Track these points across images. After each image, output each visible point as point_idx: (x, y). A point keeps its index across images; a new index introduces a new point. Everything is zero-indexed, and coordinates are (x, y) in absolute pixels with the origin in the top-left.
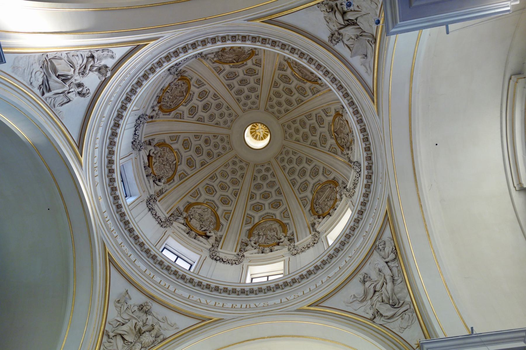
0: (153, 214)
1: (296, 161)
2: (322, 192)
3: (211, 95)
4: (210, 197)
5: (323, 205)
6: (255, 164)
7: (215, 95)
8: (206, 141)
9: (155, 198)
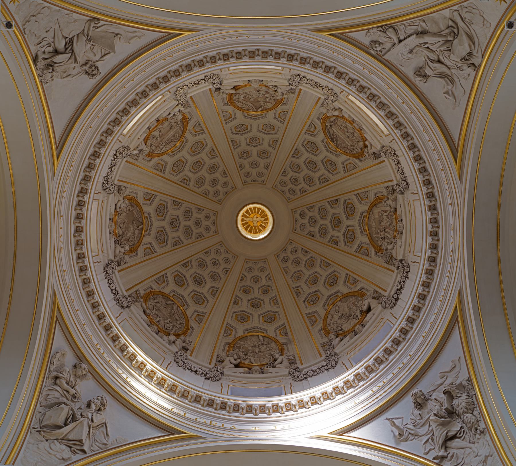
0: (313, 375)
1: (296, 172)
3: (182, 270)
5: (354, 139)
6: (293, 232)
7: (185, 265)
9: (294, 368)
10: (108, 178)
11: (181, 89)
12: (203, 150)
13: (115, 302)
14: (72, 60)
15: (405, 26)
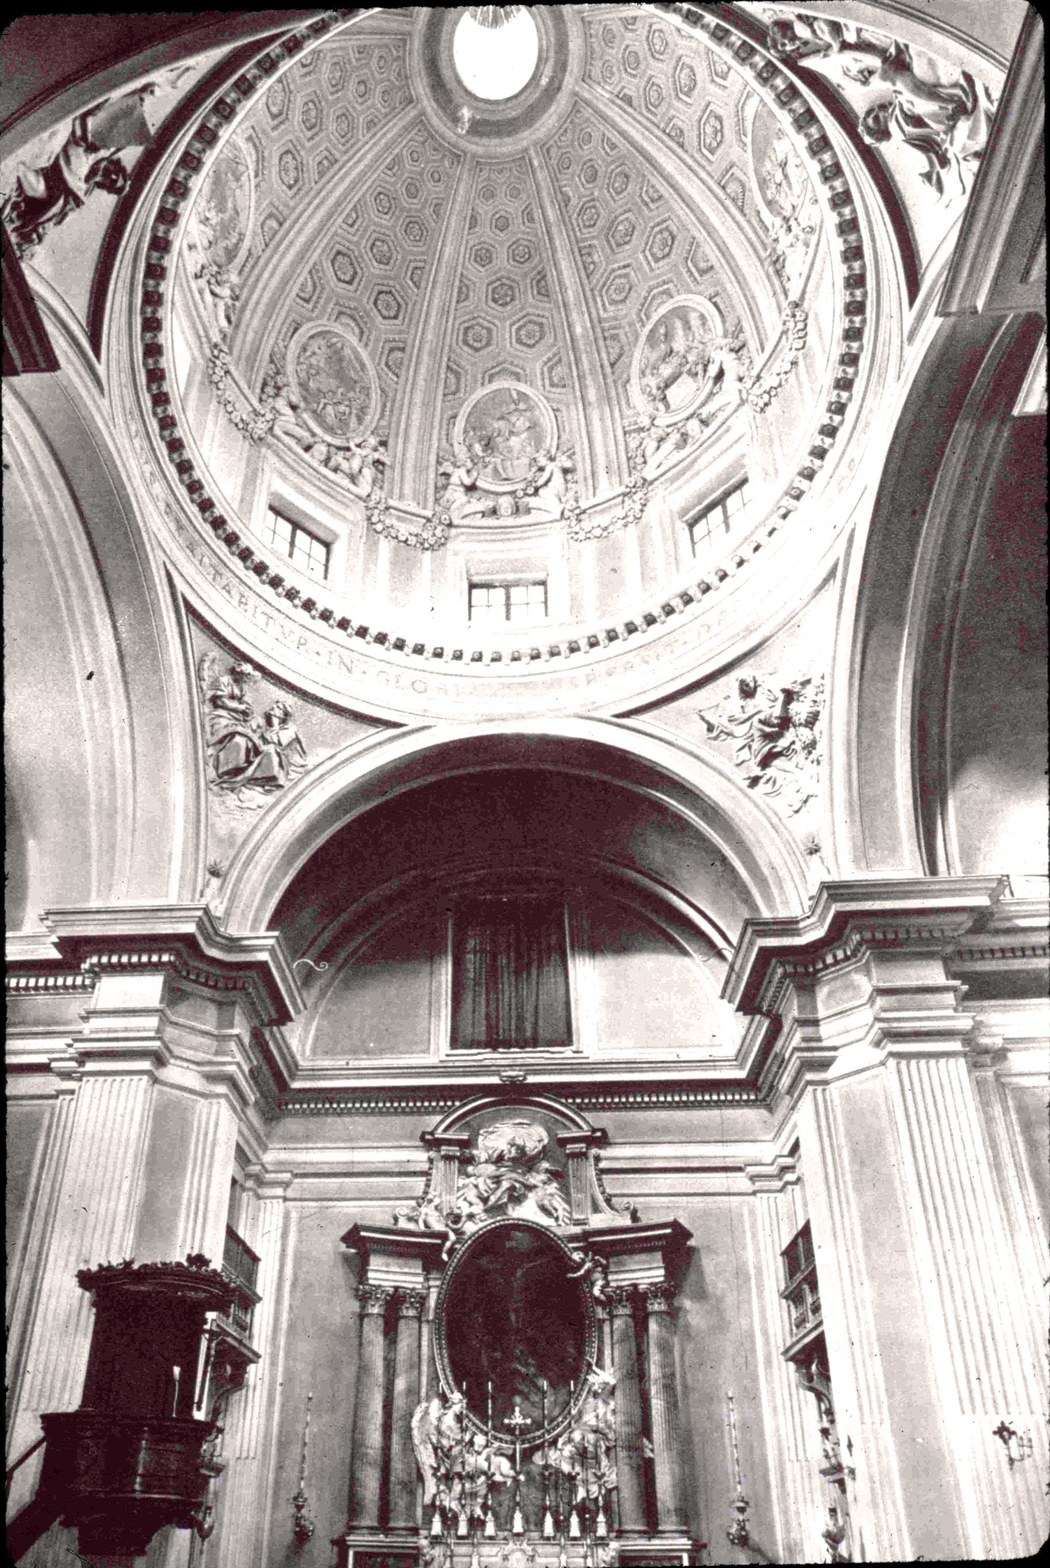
14: (72, 204)
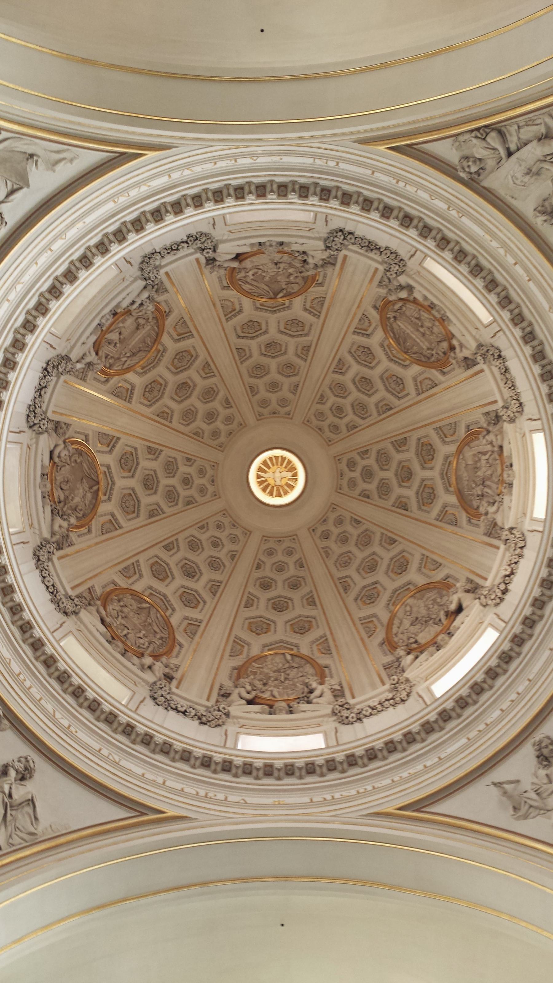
2: (405, 341)
3: (164, 555)
4: (385, 598)
6: (337, 492)
8: (266, 585)
9: (341, 704)
10: (36, 408)
11: (149, 258)
12: (191, 364)
13: (52, 606)
15: (519, 127)
